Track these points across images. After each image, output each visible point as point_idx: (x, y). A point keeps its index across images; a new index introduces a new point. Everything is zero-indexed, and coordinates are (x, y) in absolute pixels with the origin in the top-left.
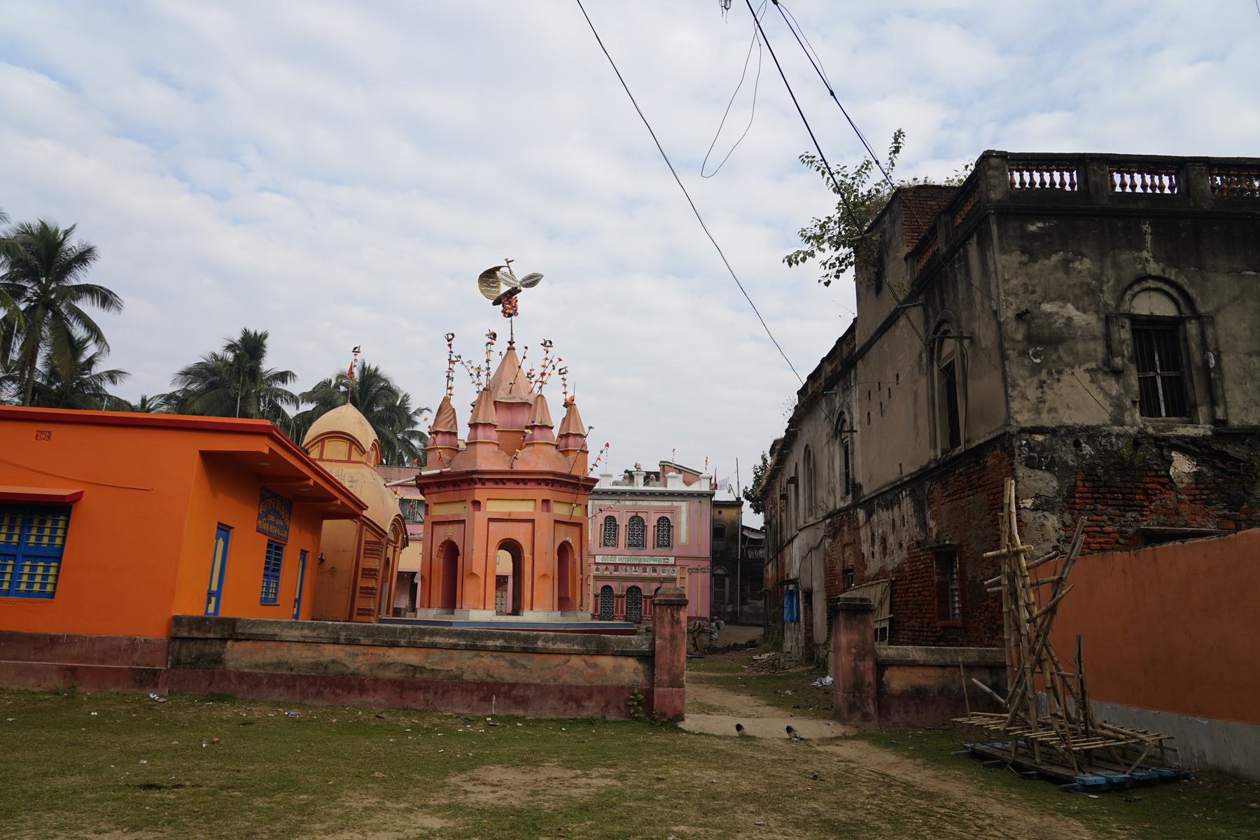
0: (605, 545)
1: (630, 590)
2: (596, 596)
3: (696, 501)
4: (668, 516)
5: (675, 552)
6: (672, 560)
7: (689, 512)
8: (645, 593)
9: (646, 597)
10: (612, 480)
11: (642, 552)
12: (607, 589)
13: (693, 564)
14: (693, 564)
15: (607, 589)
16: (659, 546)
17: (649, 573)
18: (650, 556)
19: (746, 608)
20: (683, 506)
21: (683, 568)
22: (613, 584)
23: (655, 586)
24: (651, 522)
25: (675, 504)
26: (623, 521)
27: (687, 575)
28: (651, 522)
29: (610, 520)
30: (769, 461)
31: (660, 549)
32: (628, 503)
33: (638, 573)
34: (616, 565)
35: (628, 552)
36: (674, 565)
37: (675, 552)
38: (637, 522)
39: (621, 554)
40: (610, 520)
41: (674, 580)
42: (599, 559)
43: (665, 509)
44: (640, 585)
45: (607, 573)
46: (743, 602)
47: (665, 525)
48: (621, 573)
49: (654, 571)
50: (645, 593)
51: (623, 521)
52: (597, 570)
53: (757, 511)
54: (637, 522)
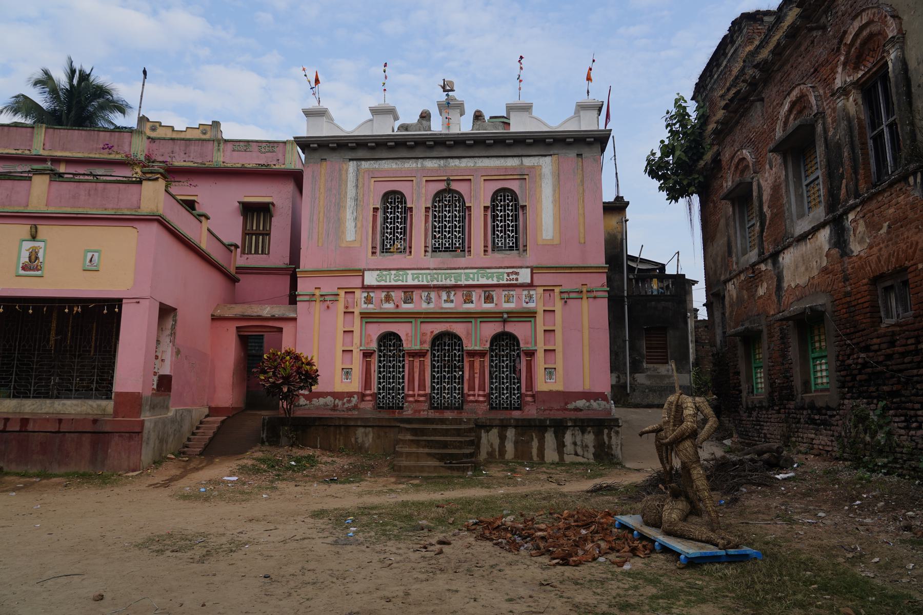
0: (385, 250)
1: (438, 339)
2: (367, 354)
3: (571, 154)
4: (514, 186)
5: (531, 258)
6: (524, 276)
7: (558, 177)
8: (470, 346)
9: (472, 354)
10: (397, 124)
11: (462, 261)
12: (389, 340)
13: (570, 282)
14: (570, 282)
15: (389, 340)
16: (495, 248)
17: (478, 304)
18: (478, 267)
19: (641, 378)
20: (546, 165)
21: (549, 290)
22: (402, 329)
23: (491, 329)
24: (479, 198)
25: (528, 162)
26: (420, 199)
27: (558, 306)
28: (479, 198)
29: (394, 202)
30: (692, 108)
31: (498, 256)
32: (430, 164)
33: (455, 303)
34: (408, 290)
35: (432, 261)
36: (531, 286)
37: (531, 258)
38: (448, 200)
39: (418, 267)
40: (394, 202)
41: (529, 316)
42: (371, 279)
43: (506, 174)
44: (458, 329)
45: (389, 307)
46: (636, 367)
47: (508, 209)
48: (420, 304)
49: (489, 299)
50: (471, 345)
51: (420, 199)
52: (368, 300)
53: (674, 196)
54: (448, 200)
